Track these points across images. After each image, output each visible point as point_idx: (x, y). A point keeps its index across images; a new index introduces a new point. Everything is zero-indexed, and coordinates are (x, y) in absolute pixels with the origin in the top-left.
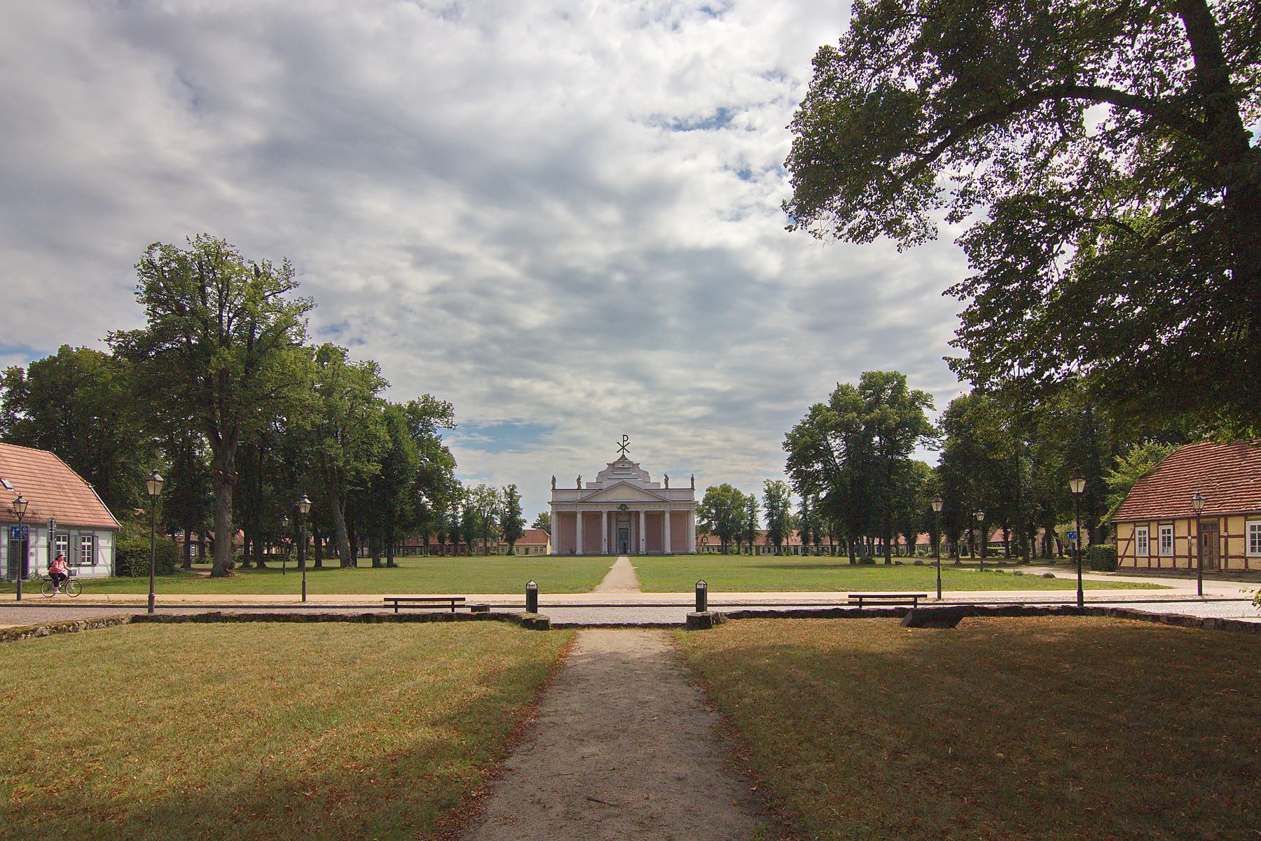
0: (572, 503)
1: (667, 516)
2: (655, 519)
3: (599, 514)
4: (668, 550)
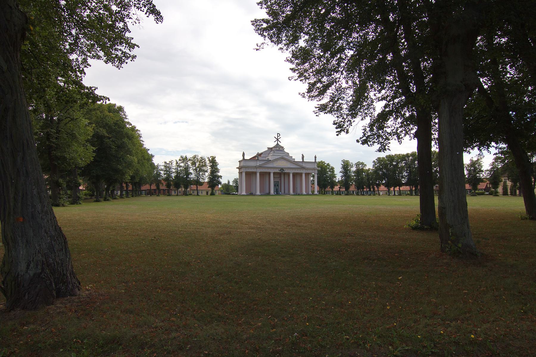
0: (256, 167)
4: (304, 193)
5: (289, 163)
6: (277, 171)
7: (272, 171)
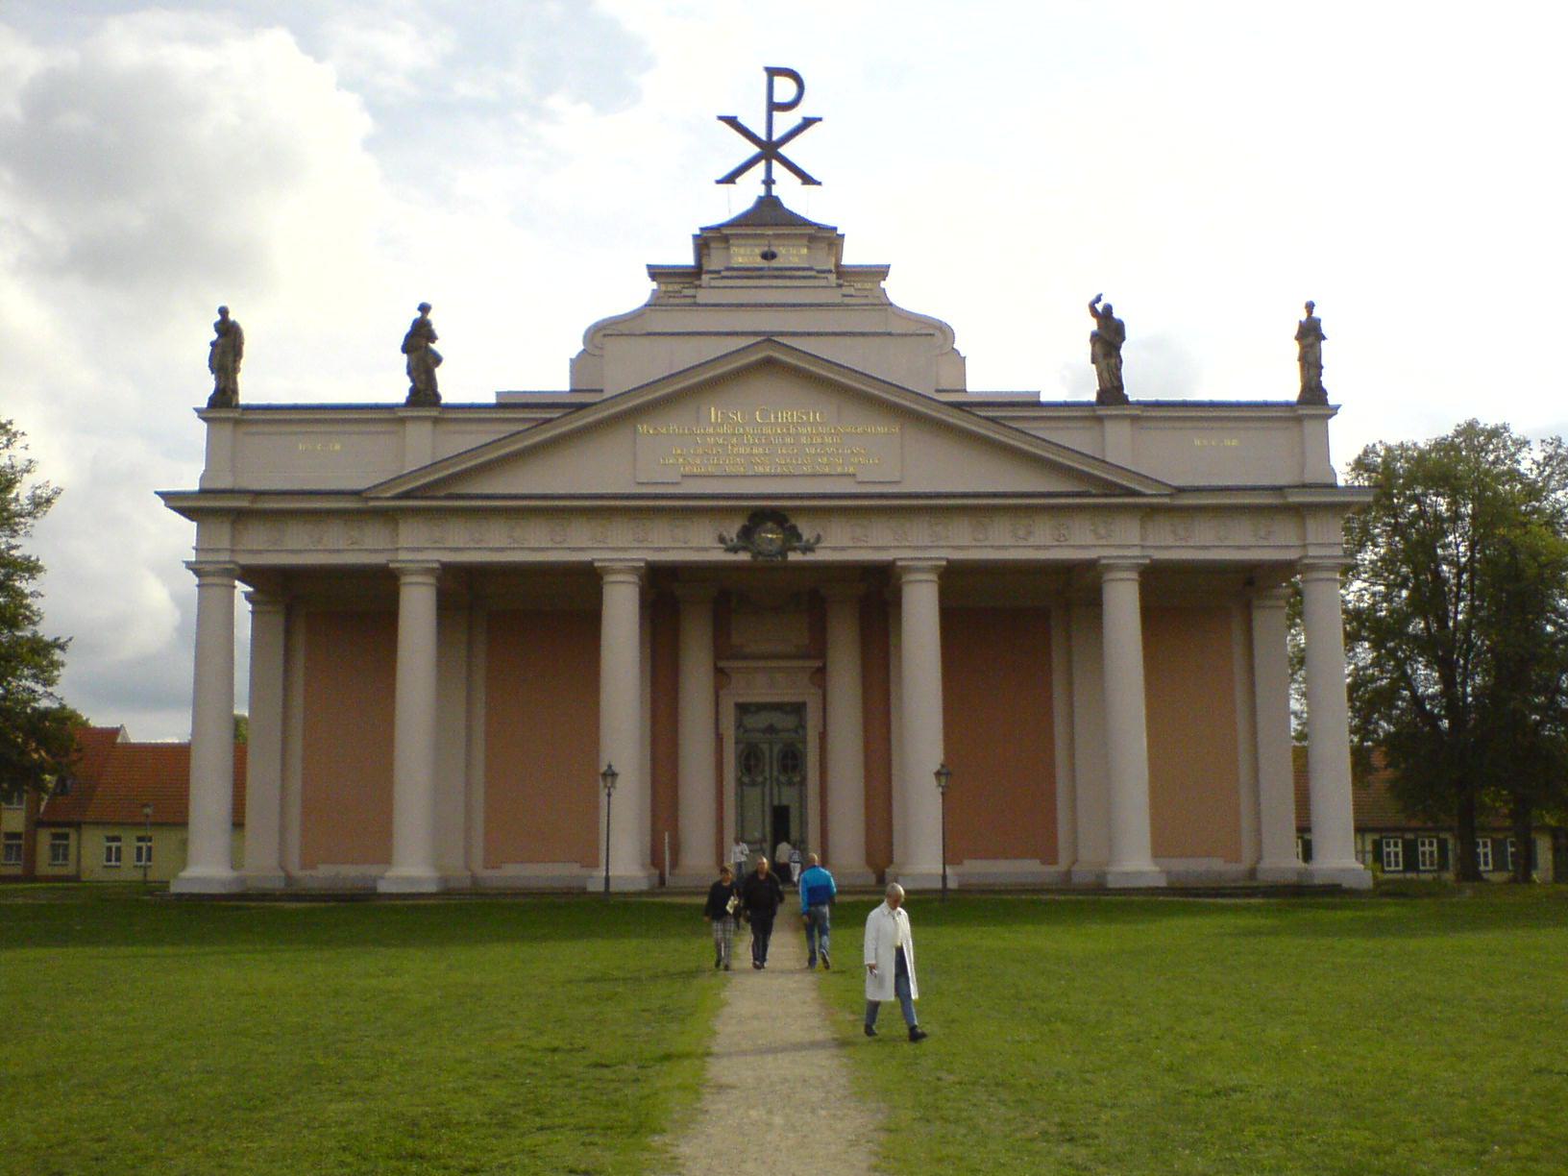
1: (1123, 603)
2: (1016, 623)
3: (582, 586)
5: (882, 429)
6: (700, 545)
7: (622, 552)
